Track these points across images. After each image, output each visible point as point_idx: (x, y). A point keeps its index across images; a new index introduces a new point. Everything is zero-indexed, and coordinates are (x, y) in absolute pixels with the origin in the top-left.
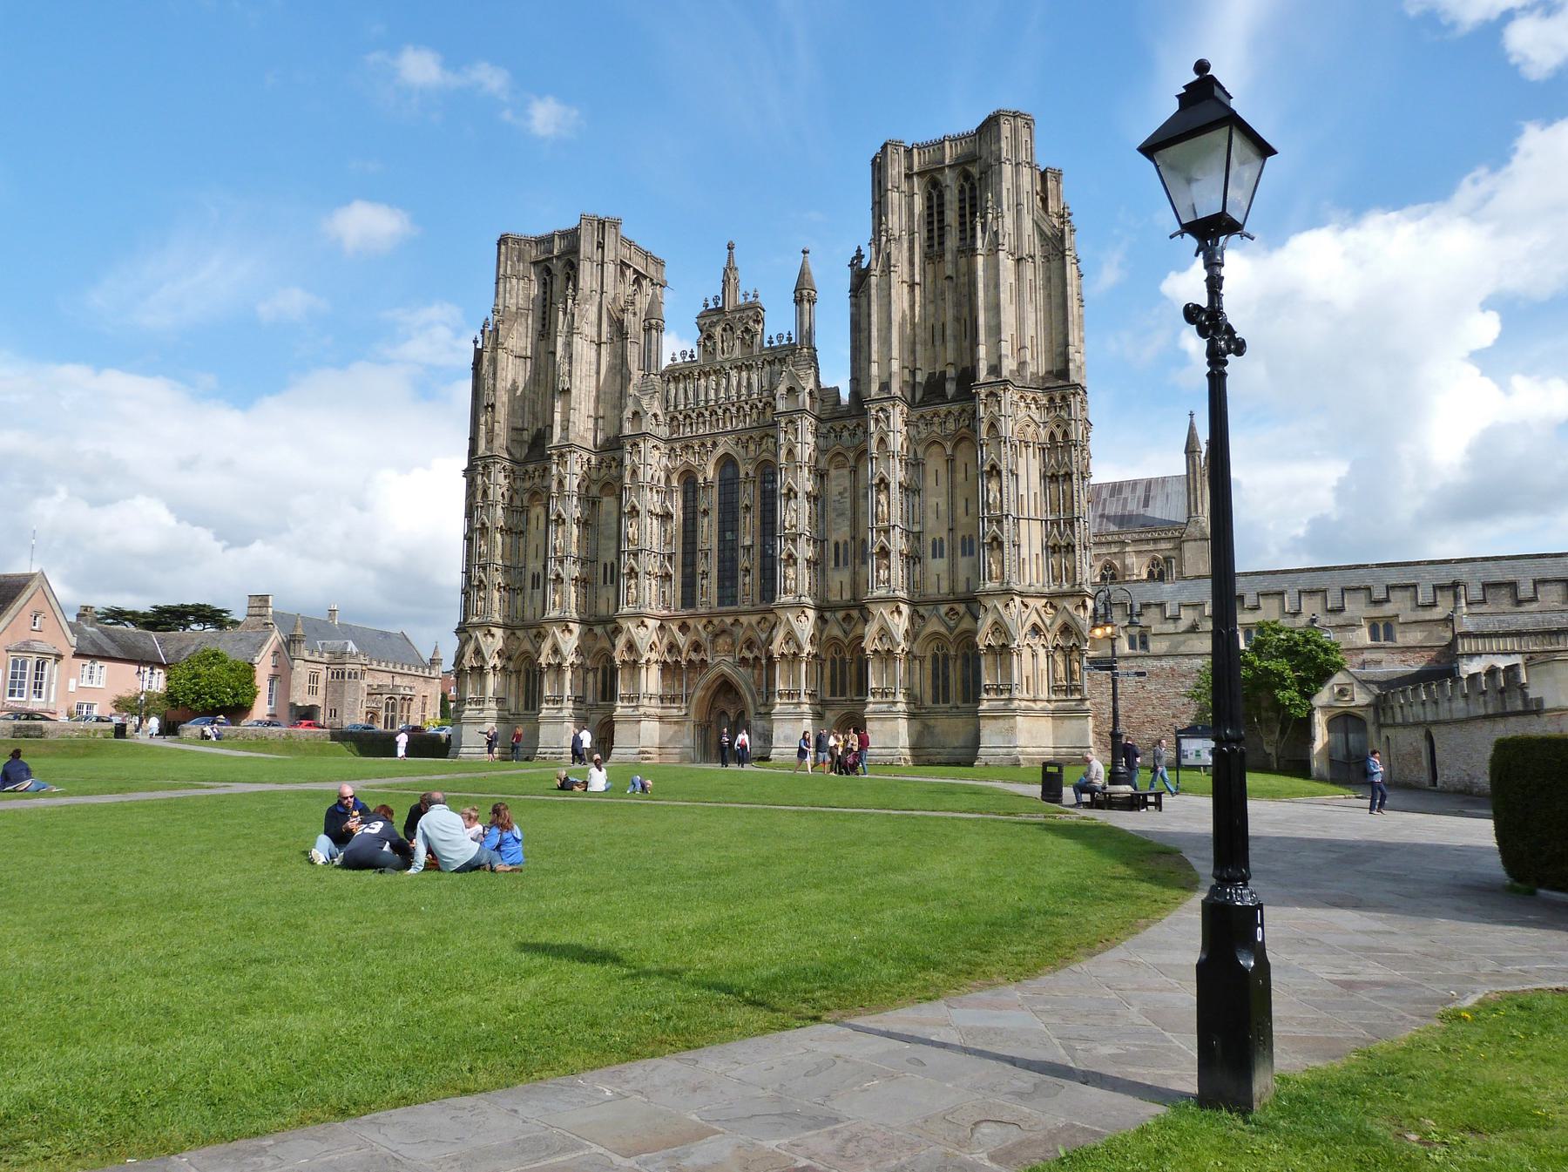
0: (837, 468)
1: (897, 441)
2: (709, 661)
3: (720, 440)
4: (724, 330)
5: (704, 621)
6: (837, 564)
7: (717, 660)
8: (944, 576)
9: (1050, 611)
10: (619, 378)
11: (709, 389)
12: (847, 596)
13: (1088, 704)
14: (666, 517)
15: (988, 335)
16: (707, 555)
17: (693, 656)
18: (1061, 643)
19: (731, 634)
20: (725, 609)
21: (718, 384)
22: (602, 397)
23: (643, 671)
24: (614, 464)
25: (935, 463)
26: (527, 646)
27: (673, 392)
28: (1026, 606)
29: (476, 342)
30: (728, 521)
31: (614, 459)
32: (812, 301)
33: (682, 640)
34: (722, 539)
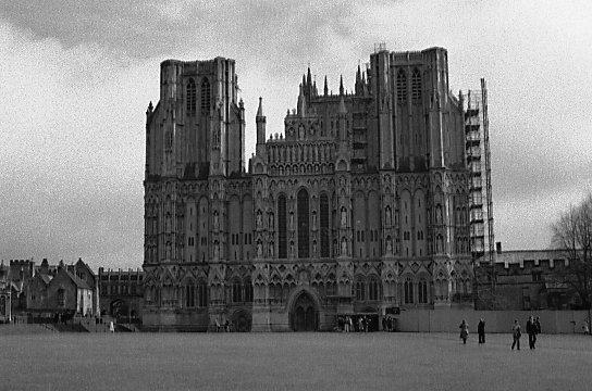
12: (364, 256)
19: (309, 272)
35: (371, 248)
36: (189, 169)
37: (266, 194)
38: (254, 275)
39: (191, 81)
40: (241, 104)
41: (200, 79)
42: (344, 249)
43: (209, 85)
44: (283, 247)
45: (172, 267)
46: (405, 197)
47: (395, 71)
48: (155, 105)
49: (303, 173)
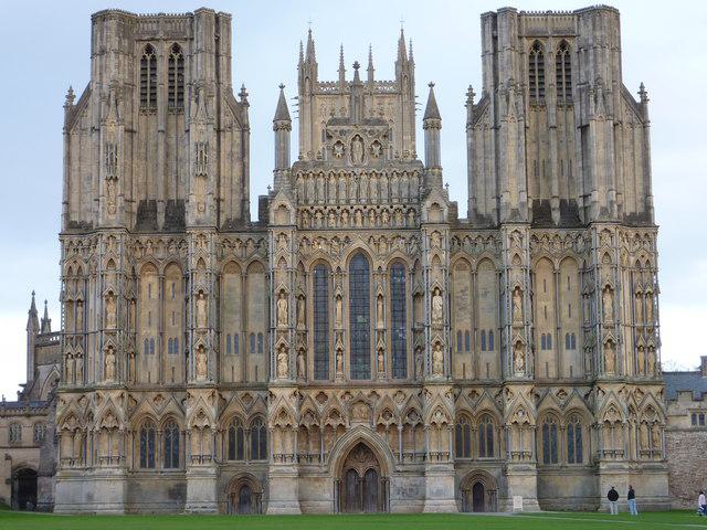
0: (459, 269)
2: (348, 426)
3: (352, 235)
4: (354, 139)
5: (342, 391)
6: (460, 349)
7: (354, 426)
9: (639, 395)
10: (237, 167)
11: (343, 191)
12: (470, 375)
13: (665, 466)
16: (341, 334)
18: (647, 419)
20: (359, 381)
21: (348, 185)
22: (222, 180)
24: (237, 245)
25: (544, 275)
29: (66, 107)
31: (238, 240)
32: (439, 128)
33: (321, 408)
34: (353, 321)
35: (482, 364)
36: (145, 213)
37: (291, 262)
38: (272, 409)
39: (149, 49)
40: (243, 95)
41: (167, 46)
42: (438, 364)
43: (181, 60)
45: (118, 393)
46: (544, 275)
47: (528, 44)
48: (78, 94)
49: (359, 225)
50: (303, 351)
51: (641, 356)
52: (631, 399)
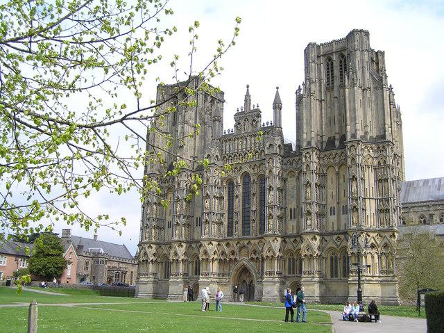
1: (314, 166)
8: (335, 223)
11: (239, 145)
12: (295, 232)
14: (221, 198)
15: (351, 121)
17: (232, 257)
19: (248, 248)
23: (211, 263)
25: (331, 175)
26: (165, 252)
27: (224, 146)
28: (369, 236)
30: (246, 200)
33: (227, 250)
34: (244, 208)
44: (230, 226)
46: (331, 175)
50: (222, 223)
51: (382, 215)
52: (372, 241)
